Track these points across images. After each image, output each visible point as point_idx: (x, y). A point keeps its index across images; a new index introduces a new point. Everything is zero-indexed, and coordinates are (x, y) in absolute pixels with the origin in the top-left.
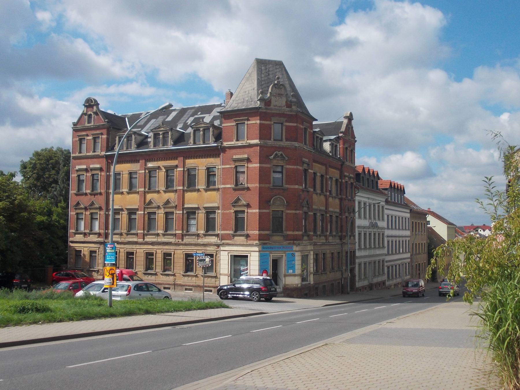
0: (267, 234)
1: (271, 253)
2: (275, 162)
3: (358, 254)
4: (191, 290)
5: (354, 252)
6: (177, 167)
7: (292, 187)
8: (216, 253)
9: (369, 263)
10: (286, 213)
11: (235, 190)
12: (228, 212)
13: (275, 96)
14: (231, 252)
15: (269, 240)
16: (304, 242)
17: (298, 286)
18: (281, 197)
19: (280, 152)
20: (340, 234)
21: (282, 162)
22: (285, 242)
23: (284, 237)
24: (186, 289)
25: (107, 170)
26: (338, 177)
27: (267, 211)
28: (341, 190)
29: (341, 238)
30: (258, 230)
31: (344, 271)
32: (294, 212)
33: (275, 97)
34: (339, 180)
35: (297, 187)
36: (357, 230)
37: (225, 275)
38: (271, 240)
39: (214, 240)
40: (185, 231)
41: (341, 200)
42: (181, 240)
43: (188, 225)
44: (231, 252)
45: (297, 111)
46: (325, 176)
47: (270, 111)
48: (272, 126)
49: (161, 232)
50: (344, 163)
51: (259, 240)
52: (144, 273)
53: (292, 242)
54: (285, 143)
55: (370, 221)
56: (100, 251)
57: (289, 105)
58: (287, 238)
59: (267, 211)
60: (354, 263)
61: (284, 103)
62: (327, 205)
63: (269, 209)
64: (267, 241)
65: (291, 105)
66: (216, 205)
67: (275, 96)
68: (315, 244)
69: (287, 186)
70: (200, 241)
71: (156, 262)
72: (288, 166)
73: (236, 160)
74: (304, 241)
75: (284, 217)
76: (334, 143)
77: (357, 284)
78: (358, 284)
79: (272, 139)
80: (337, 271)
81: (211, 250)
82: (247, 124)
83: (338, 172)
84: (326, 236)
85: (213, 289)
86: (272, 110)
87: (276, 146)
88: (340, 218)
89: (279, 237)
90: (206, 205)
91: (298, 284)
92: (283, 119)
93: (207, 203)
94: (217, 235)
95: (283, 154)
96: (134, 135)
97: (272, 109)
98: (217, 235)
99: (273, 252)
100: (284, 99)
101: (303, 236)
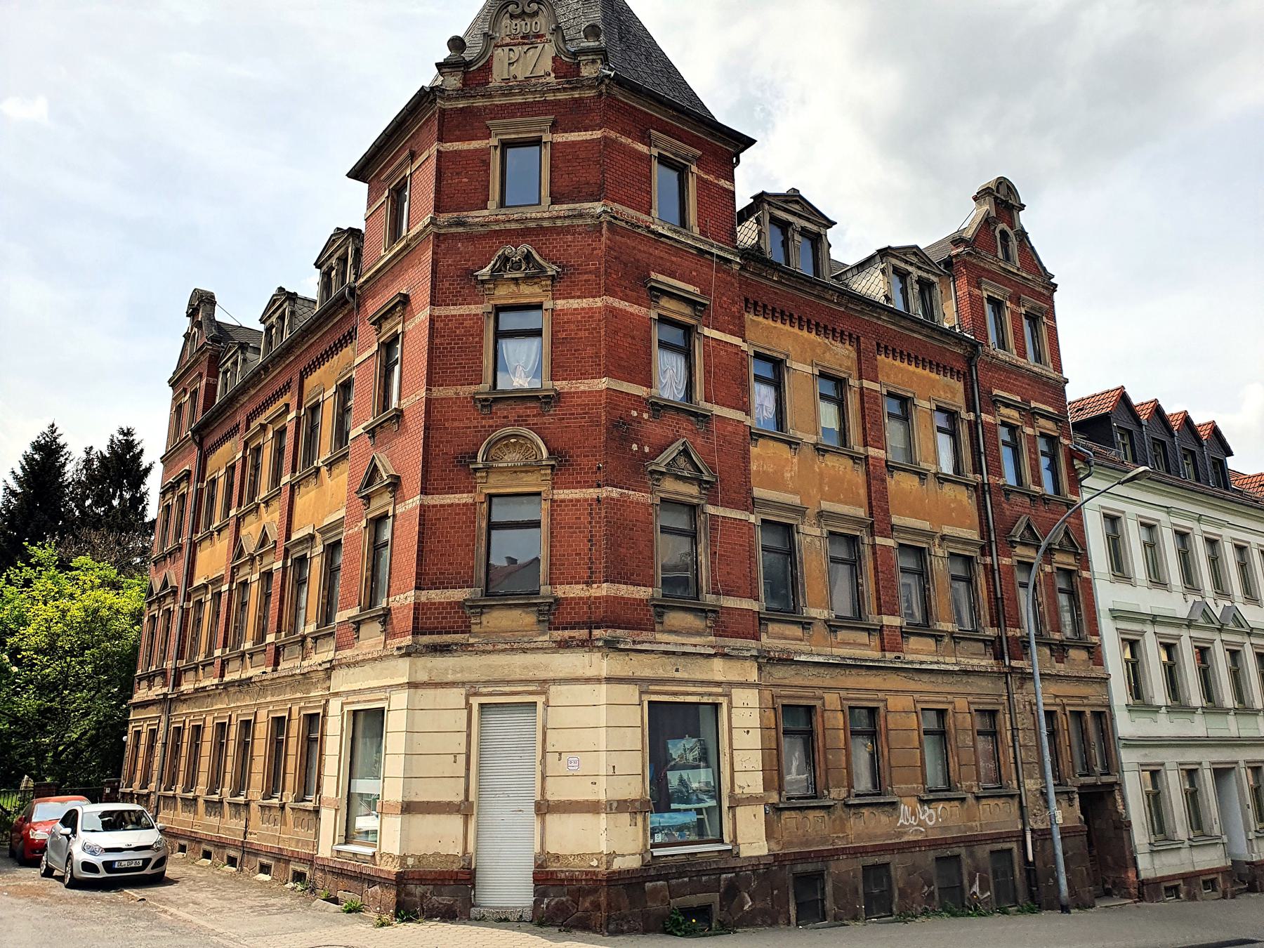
0: (460, 605)
1: (475, 694)
2: (504, 294)
3: (1125, 725)
5: (1103, 717)
7: (583, 386)
9: (1221, 773)
13: (507, 45)
14: (355, 698)
15: (467, 629)
16: (659, 637)
17: (609, 863)
18: (524, 431)
19: (524, 248)
20: (991, 632)
21: (537, 289)
22: (546, 638)
23: (540, 613)
26: (958, 401)
27: (465, 498)
28: (976, 452)
29: (997, 648)
30: (414, 584)
31: (1029, 801)
33: (506, 49)
34: (964, 414)
35: (604, 387)
36: (1108, 628)
38: (475, 628)
41: (980, 491)
42: (269, 669)
46: (853, 382)
50: (974, 346)
53: (582, 634)
54: (546, 211)
55: (1192, 598)
59: (465, 498)
60: (1111, 764)
61: (547, 64)
62: (877, 500)
64: (458, 638)
67: (507, 45)
68: (765, 660)
72: (561, 304)
74: (663, 632)
76: (910, 269)
77: (1143, 862)
78: (1148, 866)
79: (493, 204)
80: (978, 798)
83: (959, 386)
84: (881, 630)
87: (508, 226)
88: (985, 565)
89: (516, 613)
91: (612, 856)
92: (538, 126)
95: (534, 252)
100: (550, 50)
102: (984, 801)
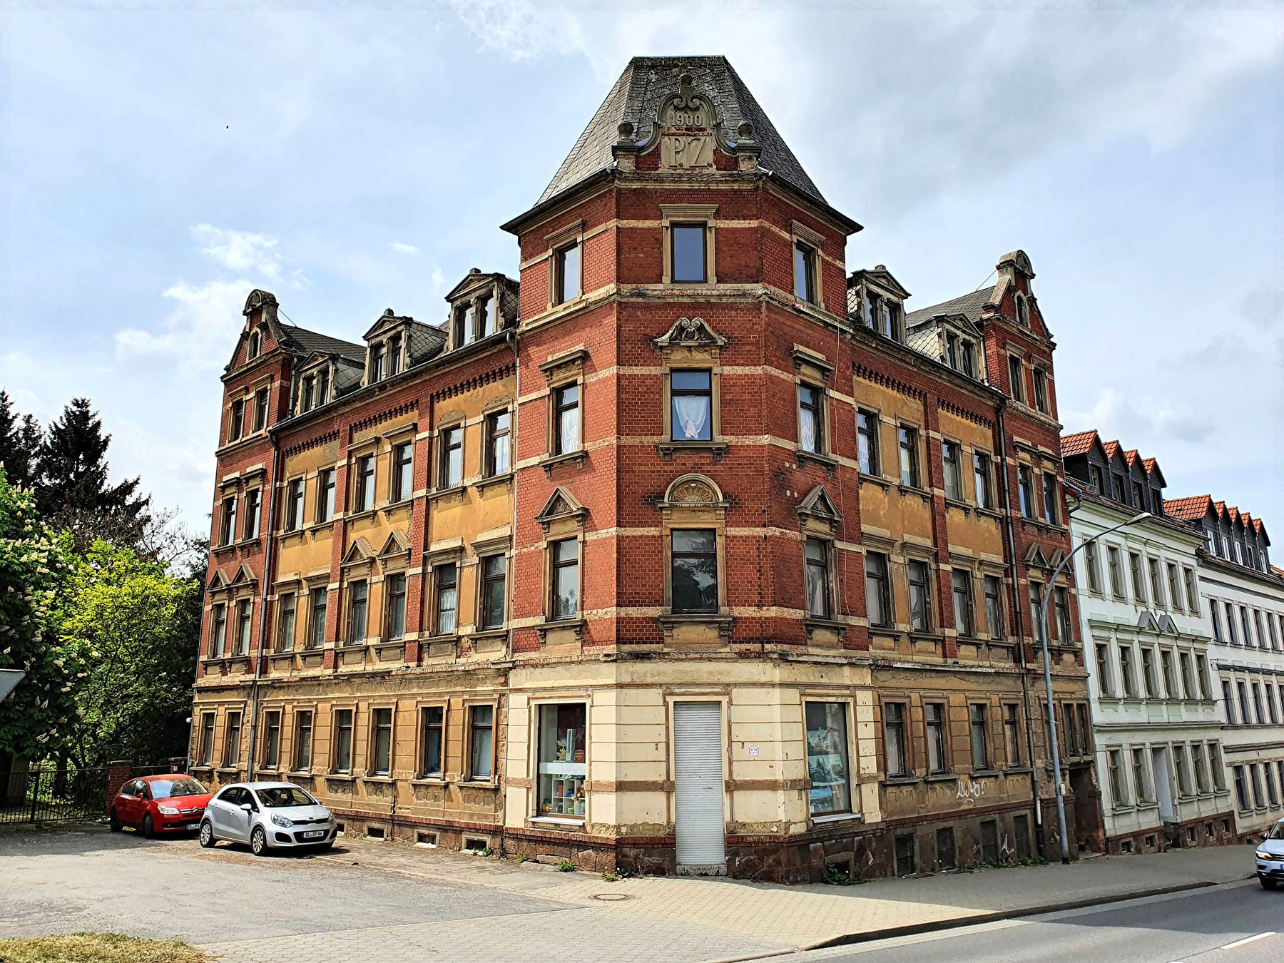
0: (655, 620)
1: (671, 694)
2: (678, 358)
3: (1099, 715)
4: (432, 839)
5: (1084, 708)
6: (415, 428)
7: (748, 441)
8: (499, 703)
9: (1156, 751)
10: (727, 537)
11: (548, 467)
12: (532, 548)
13: (673, 135)
14: (538, 695)
15: (660, 640)
16: (812, 650)
17: (787, 829)
18: (703, 478)
19: (697, 321)
20: (1012, 640)
21: (706, 356)
22: (727, 649)
23: (721, 629)
24: (422, 838)
25: (277, 474)
26: (989, 447)
27: (653, 531)
28: (1001, 490)
29: (1016, 654)
30: (615, 602)
31: (1040, 776)
32: (759, 531)
33: (673, 138)
34: (993, 458)
35: (766, 442)
36: (1086, 633)
37: (517, 783)
38: (668, 640)
39: (496, 653)
40: (427, 633)
41: (1004, 522)
42: (413, 664)
43: (439, 610)
44: (538, 695)
45: (756, 175)
46: (922, 432)
47: (657, 186)
48: (667, 236)
49: (374, 641)
50: (1003, 400)
51: (620, 641)
52: (328, 780)
53: (756, 647)
54: (714, 289)
55: (1141, 609)
56: (246, 712)
57: (727, 160)
58: (731, 631)
59: (653, 531)
60: (1088, 747)
61: (709, 157)
62: (939, 532)
63: (658, 524)
64: (654, 647)
65: (736, 159)
66: (504, 532)
67: (673, 135)
68: (878, 667)
69: (728, 439)
70: (465, 662)
71: (355, 740)
72: (727, 370)
73: (550, 370)
74: (813, 646)
75: (720, 554)
76: (958, 332)
77: (1108, 823)
78: (1113, 826)
79: (666, 279)
80: (1006, 775)
81: (486, 691)
82: (583, 241)
83: (989, 433)
84: (943, 641)
85: (488, 839)
86: (662, 181)
87: (681, 299)
88: (1008, 585)
89: (702, 628)
90: (481, 538)
91: (789, 823)
92: (703, 212)
93: (485, 529)
94: (504, 637)
95: (706, 325)
96: (333, 364)
97: (660, 180)
98: (504, 637)
99: (677, 691)
100: (711, 144)
101: (811, 625)
102: (1010, 778)
